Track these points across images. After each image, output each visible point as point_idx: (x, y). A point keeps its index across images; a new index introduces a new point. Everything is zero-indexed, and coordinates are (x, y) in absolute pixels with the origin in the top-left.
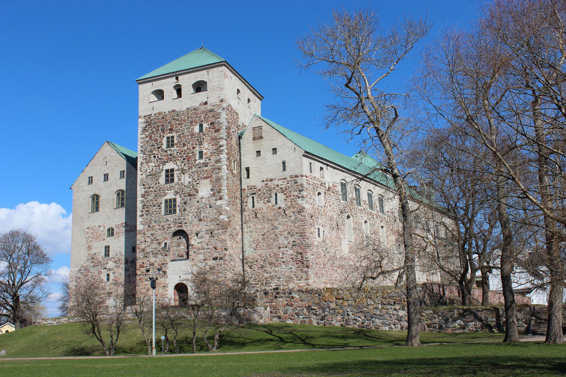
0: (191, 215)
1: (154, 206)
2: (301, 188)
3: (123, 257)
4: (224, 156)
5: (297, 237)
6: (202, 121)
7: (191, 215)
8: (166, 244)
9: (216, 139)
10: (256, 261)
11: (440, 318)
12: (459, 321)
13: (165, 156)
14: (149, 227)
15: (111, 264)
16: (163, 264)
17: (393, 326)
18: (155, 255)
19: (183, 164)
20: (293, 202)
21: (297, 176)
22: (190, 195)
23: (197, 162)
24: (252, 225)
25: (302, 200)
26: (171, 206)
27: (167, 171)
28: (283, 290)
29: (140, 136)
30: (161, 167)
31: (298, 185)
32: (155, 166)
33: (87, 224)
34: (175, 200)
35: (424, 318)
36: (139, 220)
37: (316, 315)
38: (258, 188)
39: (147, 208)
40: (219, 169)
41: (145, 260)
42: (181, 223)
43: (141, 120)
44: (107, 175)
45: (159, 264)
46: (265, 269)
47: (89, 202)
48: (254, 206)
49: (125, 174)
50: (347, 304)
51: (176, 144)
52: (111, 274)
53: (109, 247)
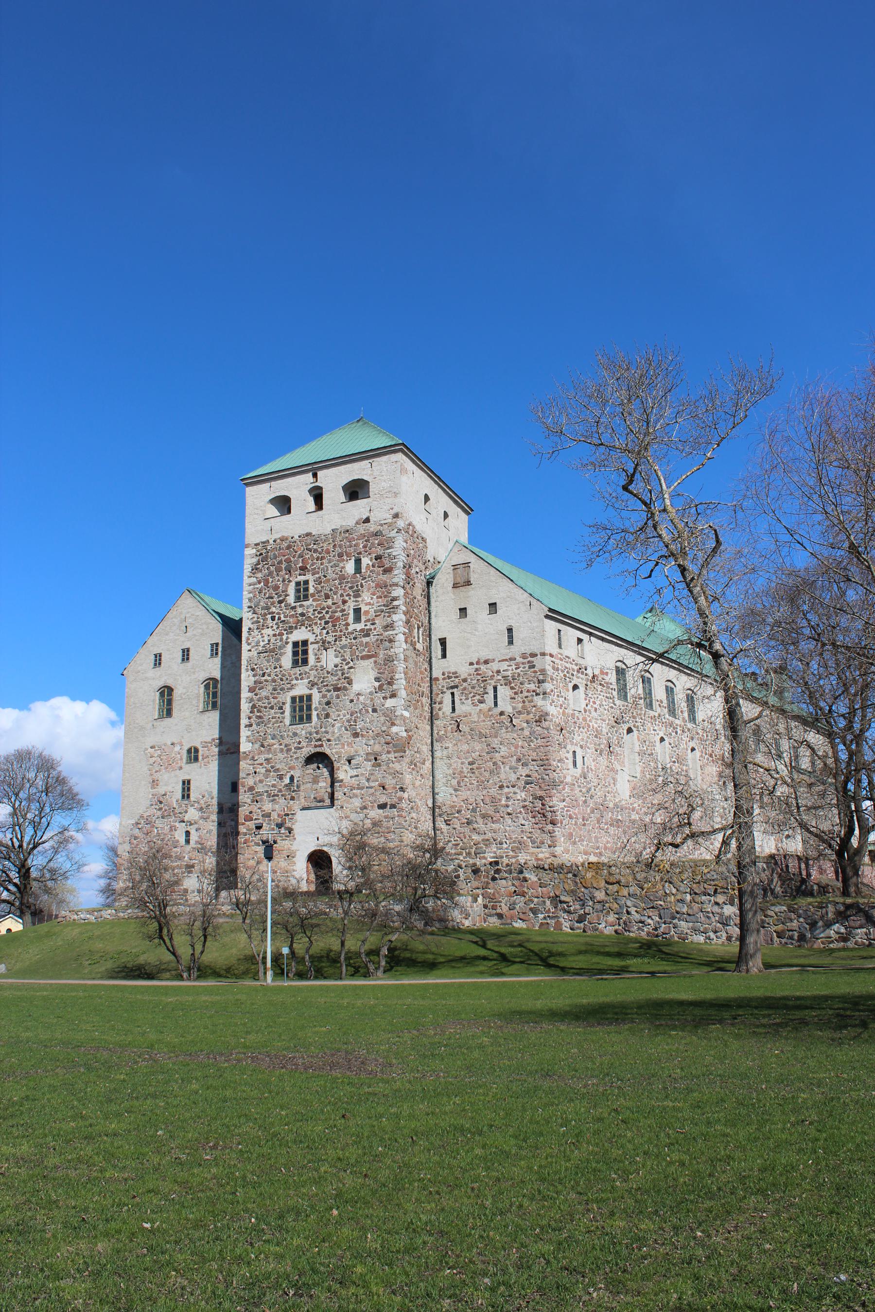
0: (338, 725)
1: (272, 708)
2: (541, 677)
3: (215, 802)
4: (399, 618)
5: (533, 766)
6: (360, 553)
7: (338, 725)
8: (292, 778)
9: (386, 586)
10: (459, 812)
11: (801, 920)
12: (836, 927)
13: (292, 616)
14: (262, 746)
15: (192, 814)
16: (287, 815)
17: (712, 935)
18: (273, 797)
19: (325, 631)
20: (527, 703)
21: (533, 655)
22: (337, 689)
23: (351, 628)
24: (450, 745)
25: (544, 699)
26: (302, 709)
27: (296, 644)
28: (507, 865)
29: (246, 580)
30: (284, 637)
31: (535, 672)
32: (275, 635)
33: (150, 740)
34: (309, 697)
35: (771, 921)
36: (244, 733)
37: (569, 912)
38: (463, 677)
39: (259, 711)
40: (391, 641)
41: (254, 808)
42: (320, 740)
43: (249, 552)
44: (188, 650)
45: (279, 815)
46: (475, 826)
47: (154, 701)
48: (454, 709)
49: (220, 649)
50: (626, 894)
51: (313, 595)
52: (193, 832)
53: (189, 782)
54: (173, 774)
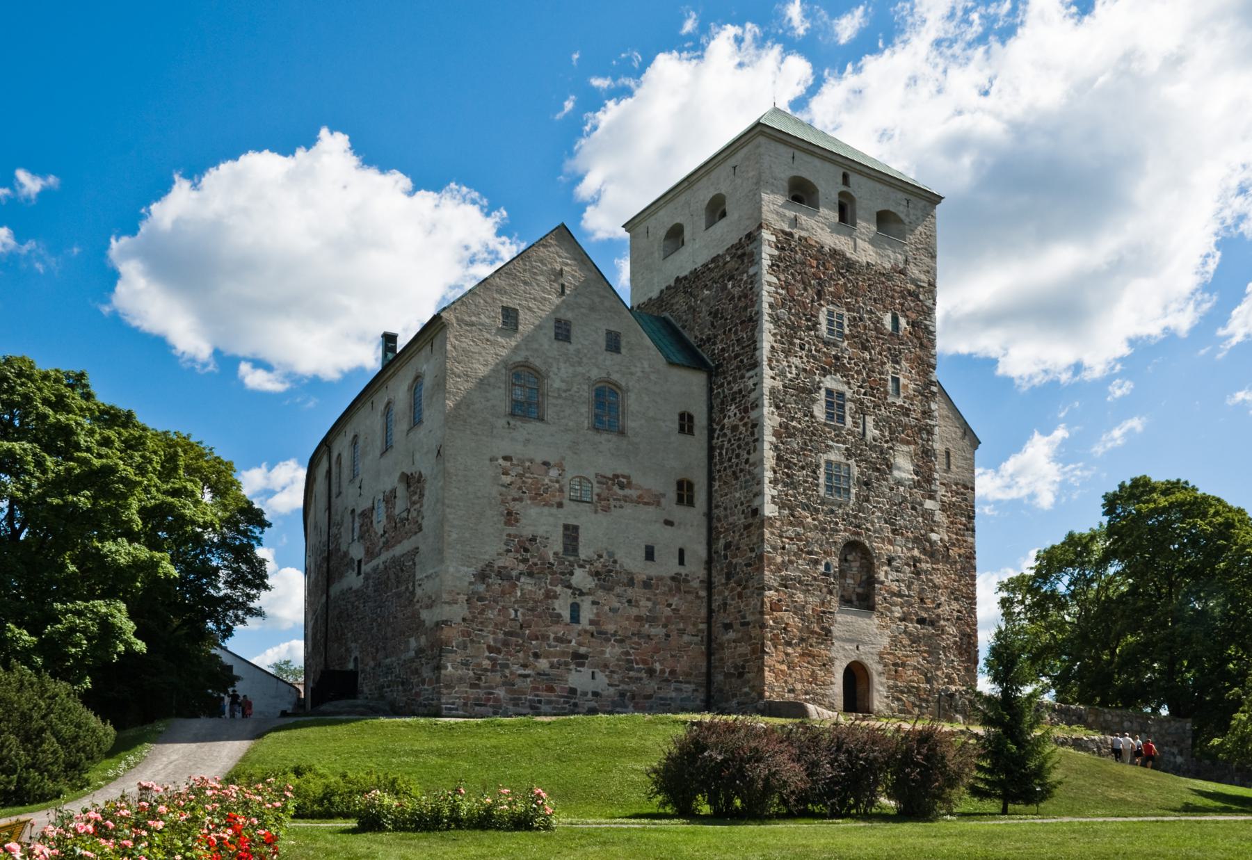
1: (803, 468)
8: (827, 566)
15: (580, 577)
23: (890, 399)
27: (829, 392)
36: (769, 491)
42: (858, 526)
53: (576, 528)
54: (546, 510)
